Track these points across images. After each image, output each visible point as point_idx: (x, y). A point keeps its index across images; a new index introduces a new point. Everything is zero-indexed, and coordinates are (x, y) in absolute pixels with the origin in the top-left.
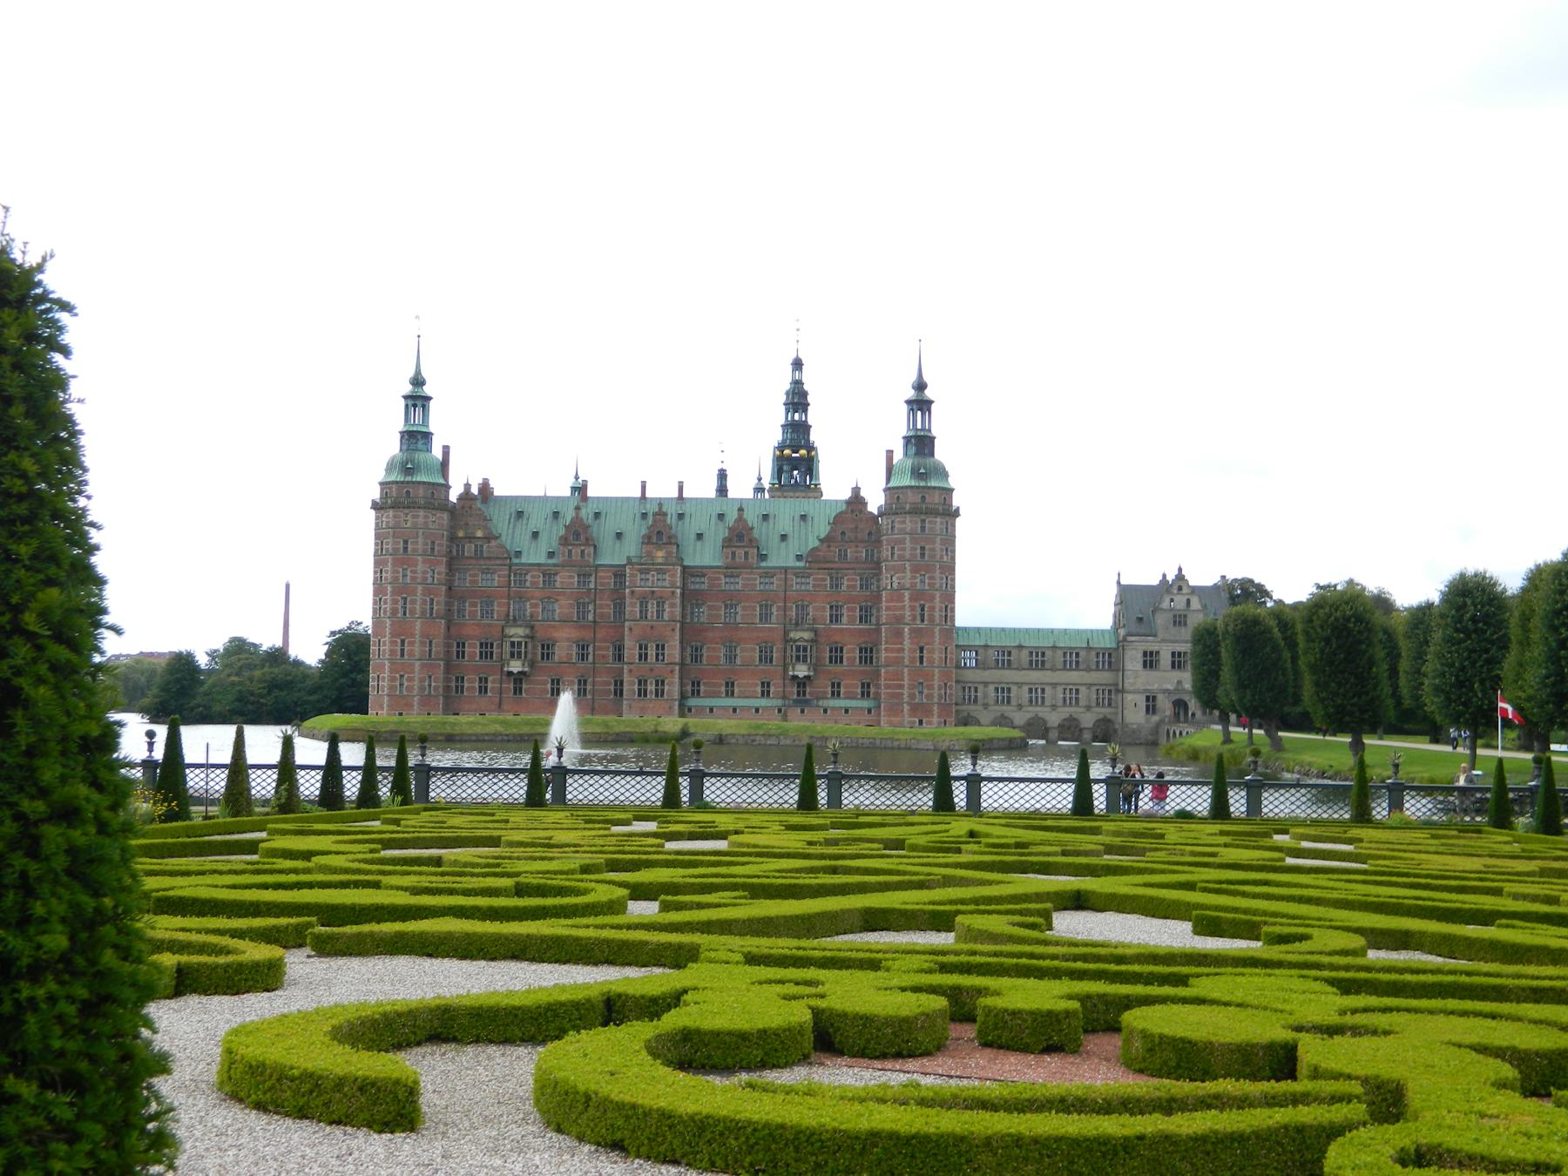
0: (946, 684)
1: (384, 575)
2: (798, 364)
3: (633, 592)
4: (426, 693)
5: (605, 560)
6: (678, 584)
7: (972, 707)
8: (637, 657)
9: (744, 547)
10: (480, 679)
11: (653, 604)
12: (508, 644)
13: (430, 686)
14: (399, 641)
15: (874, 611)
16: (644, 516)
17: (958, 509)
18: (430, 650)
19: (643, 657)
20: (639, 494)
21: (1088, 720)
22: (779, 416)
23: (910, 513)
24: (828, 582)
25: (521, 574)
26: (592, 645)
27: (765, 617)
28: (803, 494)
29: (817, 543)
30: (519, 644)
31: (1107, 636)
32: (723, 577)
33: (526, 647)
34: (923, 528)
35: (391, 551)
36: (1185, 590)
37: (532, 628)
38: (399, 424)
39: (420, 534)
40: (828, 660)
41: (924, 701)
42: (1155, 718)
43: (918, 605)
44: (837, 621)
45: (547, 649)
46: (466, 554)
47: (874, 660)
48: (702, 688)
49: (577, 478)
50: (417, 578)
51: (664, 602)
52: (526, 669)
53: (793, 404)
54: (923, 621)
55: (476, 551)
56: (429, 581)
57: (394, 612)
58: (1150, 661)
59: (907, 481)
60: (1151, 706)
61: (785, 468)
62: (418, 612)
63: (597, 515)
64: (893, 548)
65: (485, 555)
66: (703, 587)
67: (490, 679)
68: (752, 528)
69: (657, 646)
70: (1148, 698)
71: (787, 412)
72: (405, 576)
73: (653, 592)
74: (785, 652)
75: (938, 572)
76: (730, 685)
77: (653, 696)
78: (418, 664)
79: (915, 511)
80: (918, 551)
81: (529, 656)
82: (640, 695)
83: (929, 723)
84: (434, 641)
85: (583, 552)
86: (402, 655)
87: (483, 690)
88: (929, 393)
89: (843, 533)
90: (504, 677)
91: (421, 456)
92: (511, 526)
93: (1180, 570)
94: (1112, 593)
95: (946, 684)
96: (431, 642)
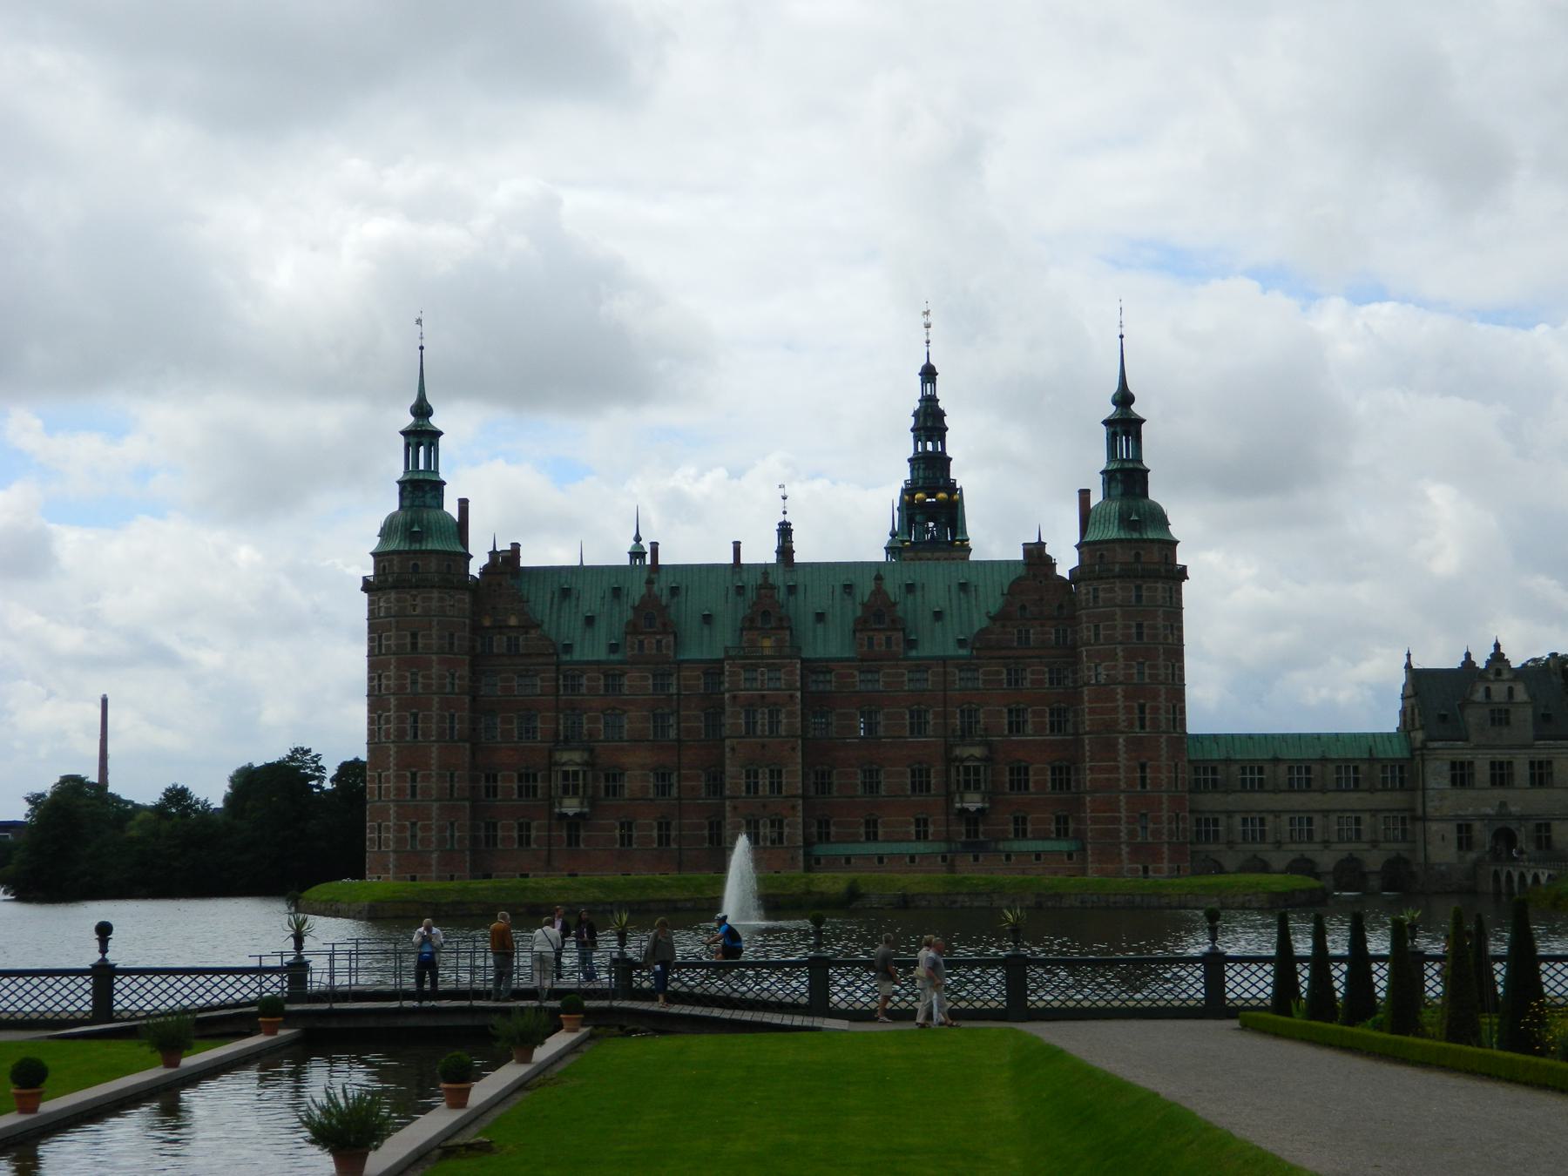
0: (1177, 815)
1: (384, 681)
2: (929, 374)
3: (734, 697)
4: (448, 847)
5: (692, 653)
6: (798, 684)
7: (1212, 847)
8: (744, 788)
9: (884, 630)
11: (763, 713)
12: (560, 775)
14: (408, 774)
15: (1070, 716)
16: (740, 590)
18: (452, 786)
19: (752, 788)
20: (730, 560)
21: (1374, 861)
22: (906, 447)
23: (1119, 577)
24: (1004, 676)
25: (573, 677)
26: (675, 774)
27: (918, 727)
28: (945, 554)
29: (985, 623)
30: (576, 773)
31: (1395, 741)
32: (856, 673)
33: (584, 779)
34: (1139, 597)
35: (394, 648)
36: (1506, 675)
37: (591, 751)
38: (395, 466)
39: (435, 623)
40: (1007, 785)
41: (1150, 839)
42: (1472, 856)
43: (1136, 705)
44: (1018, 731)
45: (614, 779)
46: (495, 650)
47: (1073, 784)
48: (833, 830)
49: (638, 539)
50: (431, 685)
51: (778, 711)
52: (586, 810)
53: (925, 429)
54: (1143, 727)
56: (448, 689)
57: (401, 733)
58: (1461, 775)
59: (1113, 533)
60: (1465, 839)
61: (918, 518)
62: (434, 733)
63: (674, 591)
64: (1097, 627)
66: (828, 688)
67: (534, 824)
68: (895, 604)
69: (772, 771)
70: (1460, 827)
71: (917, 439)
72: (414, 682)
73: (763, 697)
74: (947, 771)
75: (1162, 657)
77: (768, 844)
78: (435, 805)
79: (1126, 575)
80: (1134, 630)
81: (590, 792)
83: (1157, 871)
84: (456, 774)
85: (659, 642)
86: (414, 794)
87: (524, 841)
89: (1023, 608)
91: (431, 515)
92: (555, 607)
93: (1497, 646)
94: (1401, 678)
95: (1177, 815)
96: (452, 776)
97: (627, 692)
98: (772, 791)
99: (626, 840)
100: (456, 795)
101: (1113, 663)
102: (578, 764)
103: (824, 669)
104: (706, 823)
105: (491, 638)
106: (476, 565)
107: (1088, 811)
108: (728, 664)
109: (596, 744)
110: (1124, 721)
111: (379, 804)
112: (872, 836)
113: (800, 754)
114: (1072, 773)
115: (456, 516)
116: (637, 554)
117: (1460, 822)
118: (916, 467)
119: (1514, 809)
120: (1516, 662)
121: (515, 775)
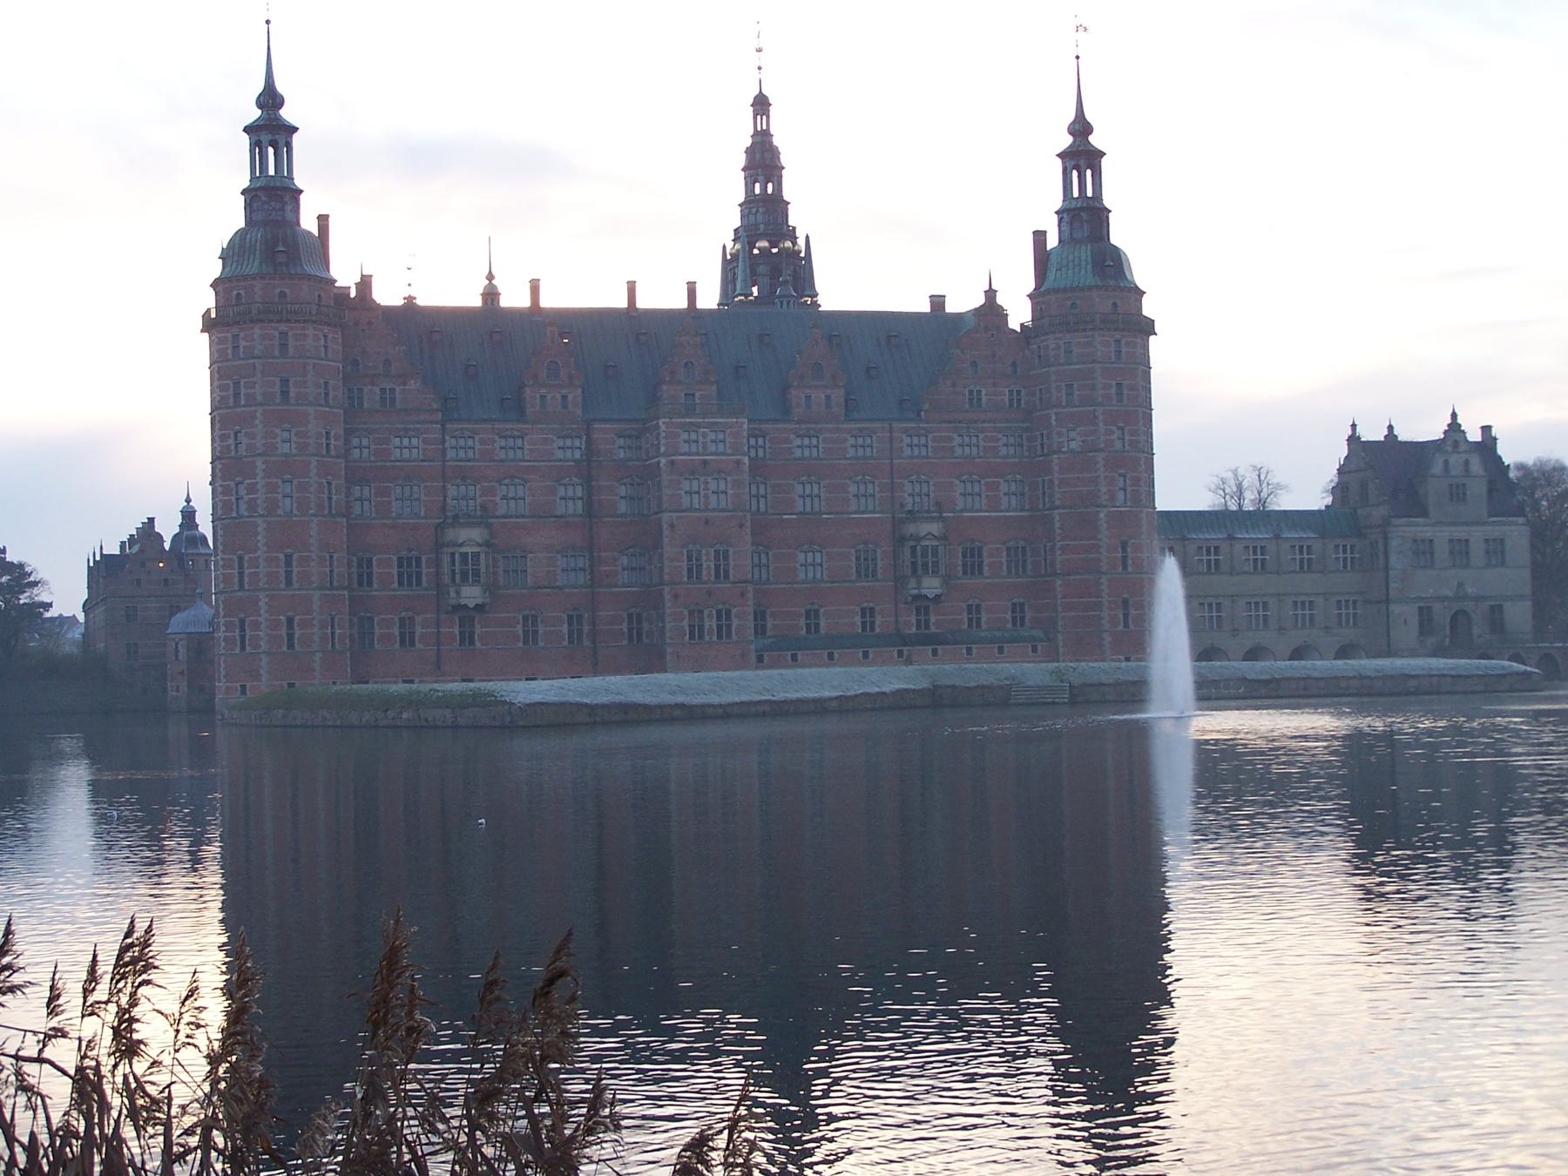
1: (245, 441)
2: (761, 105)
8: (685, 572)
10: (402, 620)
13: (333, 634)
14: (282, 556)
18: (331, 571)
19: (694, 572)
30: (476, 555)
32: (792, 436)
34: (1119, 352)
35: (259, 398)
36: (1462, 447)
37: (488, 526)
40: (960, 568)
46: (366, 405)
55: (383, 399)
62: (312, 505)
65: (398, 405)
67: (419, 619)
73: (705, 462)
77: (715, 638)
78: (317, 595)
80: (1113, 391)
82: (692, 636)
85: (564, 397)
86: (289, 583)
87: (407, 639)
88: (1095, 140)
89: (974, 364)
90: (442, 616)
93: (1454, 415)
97: (527, 458)
98: (717, 576)
99: (530, 636)
100: (335, 584)
101: (1093, 428)
102: (479, 545)
103: (757, 432)
104: (625, 615)
105: (361, 390)
107: (1059, 596)
108: (664, 423)
109: (493, 520)
110: (1105, 493)
111: (240, 594)
113: (749, 531)
114: (1029, 554)
115: (317, 235)
117: (1422, 604)
118: (754, 210)
119: (1469, 590)
121: (395, 558)
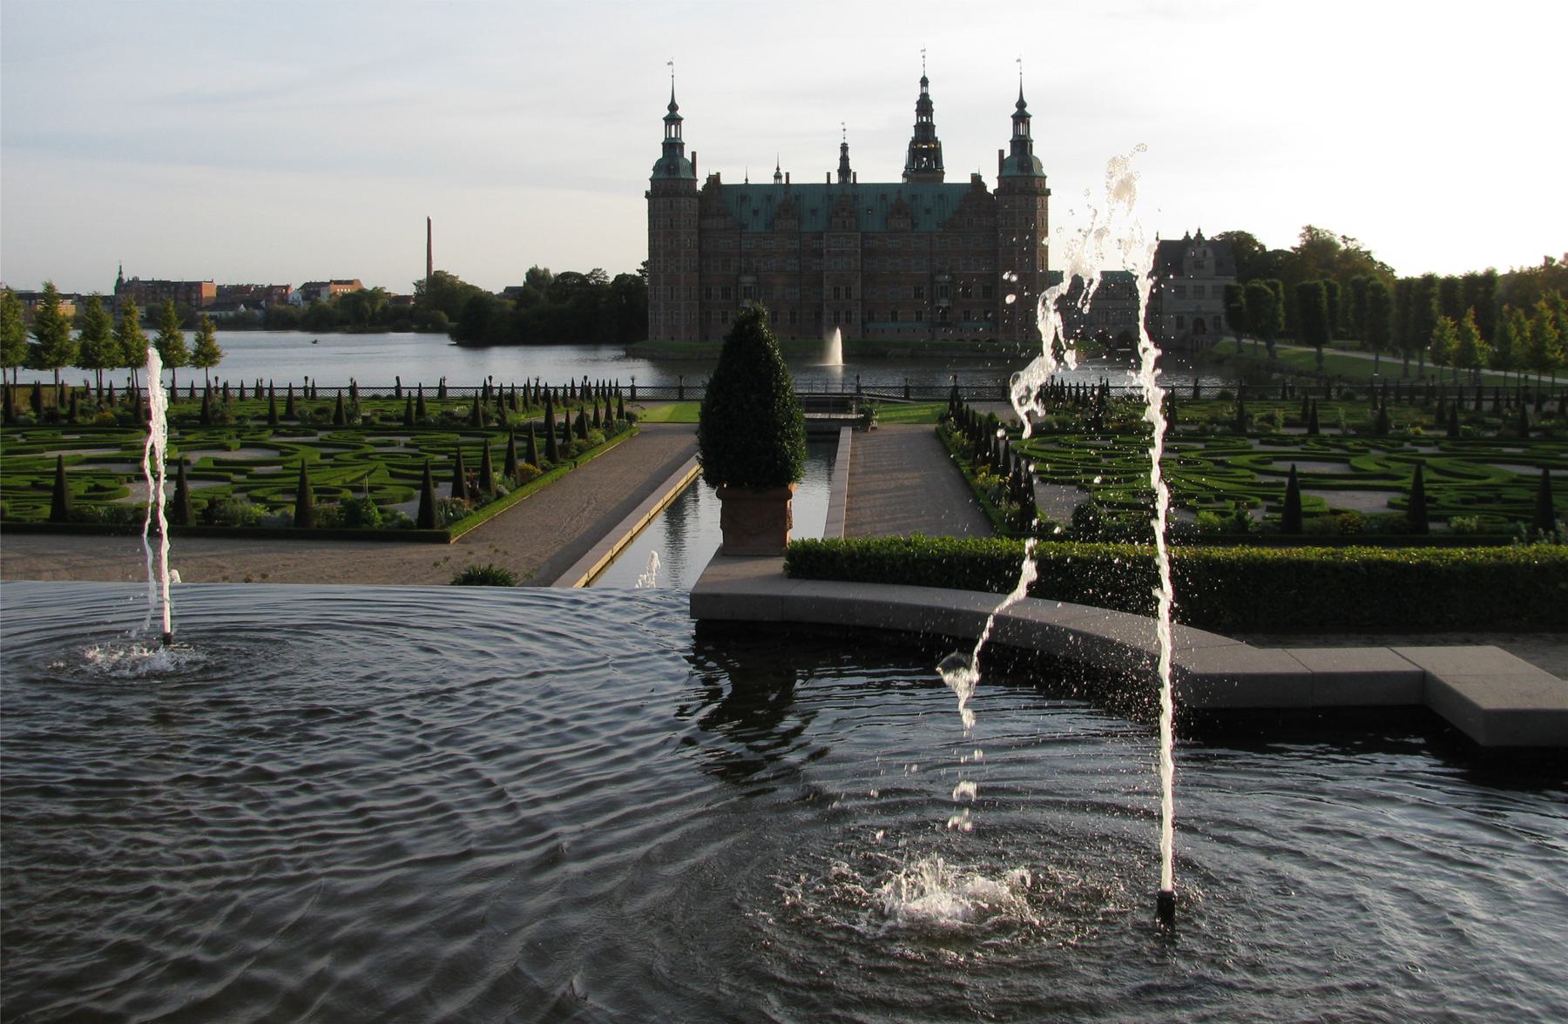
2: (924, 82)
3: (828, 252)
17: (1049, 191)
19: (837, 296)
20: (825, 182)
22: (911, 118)
30: (750, 288)
36: (1203, 245)
42: (1183, 331)
49: (778, 169)
59: (1015, 172)
60: (1180, 323)
63: (797, 198)
76: (894, 314)
86: (672, 298)
87: (725, 320)
93: (1199, 230)
106: (700, 184)
112: (894, 319)
115: (690, 161)
116: (778, 176)
119: (1204, 309)
120: (1207, 238)
